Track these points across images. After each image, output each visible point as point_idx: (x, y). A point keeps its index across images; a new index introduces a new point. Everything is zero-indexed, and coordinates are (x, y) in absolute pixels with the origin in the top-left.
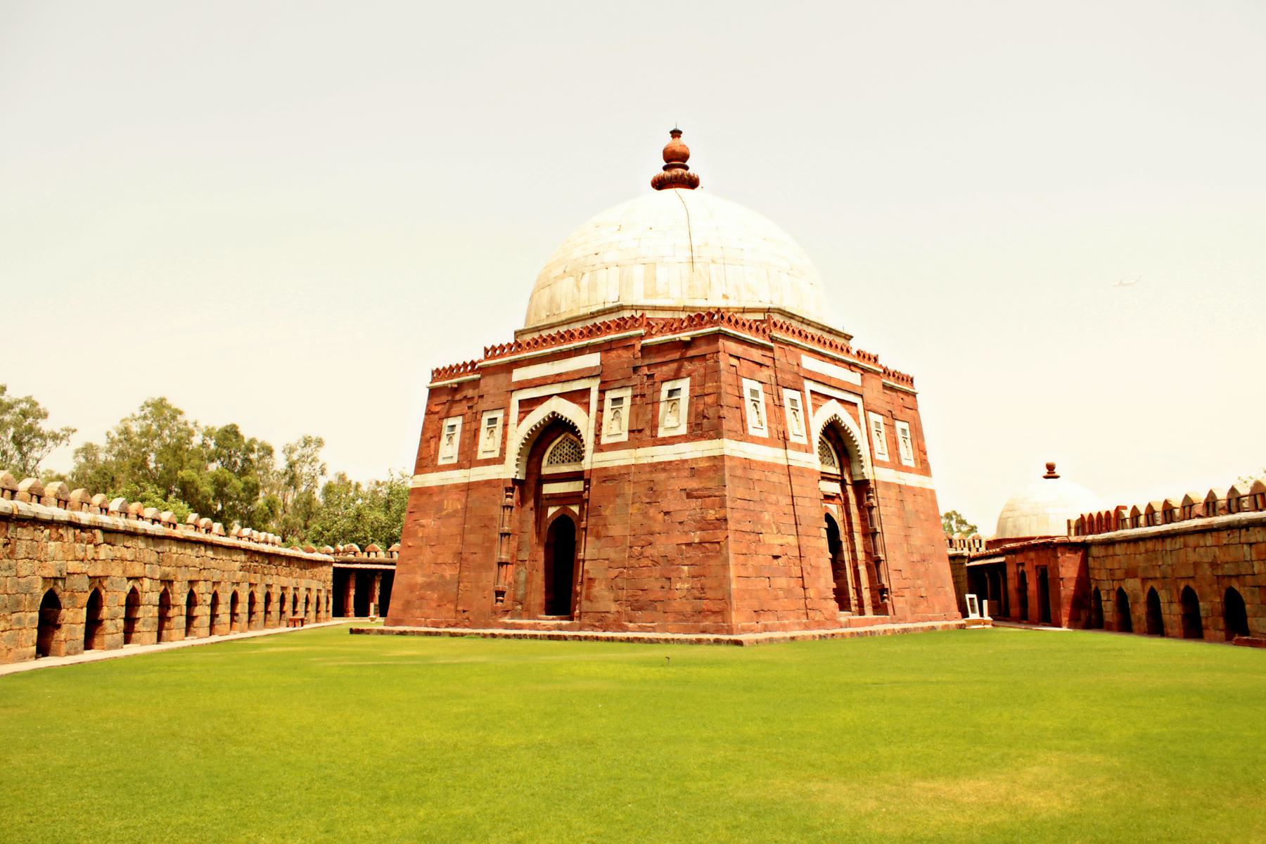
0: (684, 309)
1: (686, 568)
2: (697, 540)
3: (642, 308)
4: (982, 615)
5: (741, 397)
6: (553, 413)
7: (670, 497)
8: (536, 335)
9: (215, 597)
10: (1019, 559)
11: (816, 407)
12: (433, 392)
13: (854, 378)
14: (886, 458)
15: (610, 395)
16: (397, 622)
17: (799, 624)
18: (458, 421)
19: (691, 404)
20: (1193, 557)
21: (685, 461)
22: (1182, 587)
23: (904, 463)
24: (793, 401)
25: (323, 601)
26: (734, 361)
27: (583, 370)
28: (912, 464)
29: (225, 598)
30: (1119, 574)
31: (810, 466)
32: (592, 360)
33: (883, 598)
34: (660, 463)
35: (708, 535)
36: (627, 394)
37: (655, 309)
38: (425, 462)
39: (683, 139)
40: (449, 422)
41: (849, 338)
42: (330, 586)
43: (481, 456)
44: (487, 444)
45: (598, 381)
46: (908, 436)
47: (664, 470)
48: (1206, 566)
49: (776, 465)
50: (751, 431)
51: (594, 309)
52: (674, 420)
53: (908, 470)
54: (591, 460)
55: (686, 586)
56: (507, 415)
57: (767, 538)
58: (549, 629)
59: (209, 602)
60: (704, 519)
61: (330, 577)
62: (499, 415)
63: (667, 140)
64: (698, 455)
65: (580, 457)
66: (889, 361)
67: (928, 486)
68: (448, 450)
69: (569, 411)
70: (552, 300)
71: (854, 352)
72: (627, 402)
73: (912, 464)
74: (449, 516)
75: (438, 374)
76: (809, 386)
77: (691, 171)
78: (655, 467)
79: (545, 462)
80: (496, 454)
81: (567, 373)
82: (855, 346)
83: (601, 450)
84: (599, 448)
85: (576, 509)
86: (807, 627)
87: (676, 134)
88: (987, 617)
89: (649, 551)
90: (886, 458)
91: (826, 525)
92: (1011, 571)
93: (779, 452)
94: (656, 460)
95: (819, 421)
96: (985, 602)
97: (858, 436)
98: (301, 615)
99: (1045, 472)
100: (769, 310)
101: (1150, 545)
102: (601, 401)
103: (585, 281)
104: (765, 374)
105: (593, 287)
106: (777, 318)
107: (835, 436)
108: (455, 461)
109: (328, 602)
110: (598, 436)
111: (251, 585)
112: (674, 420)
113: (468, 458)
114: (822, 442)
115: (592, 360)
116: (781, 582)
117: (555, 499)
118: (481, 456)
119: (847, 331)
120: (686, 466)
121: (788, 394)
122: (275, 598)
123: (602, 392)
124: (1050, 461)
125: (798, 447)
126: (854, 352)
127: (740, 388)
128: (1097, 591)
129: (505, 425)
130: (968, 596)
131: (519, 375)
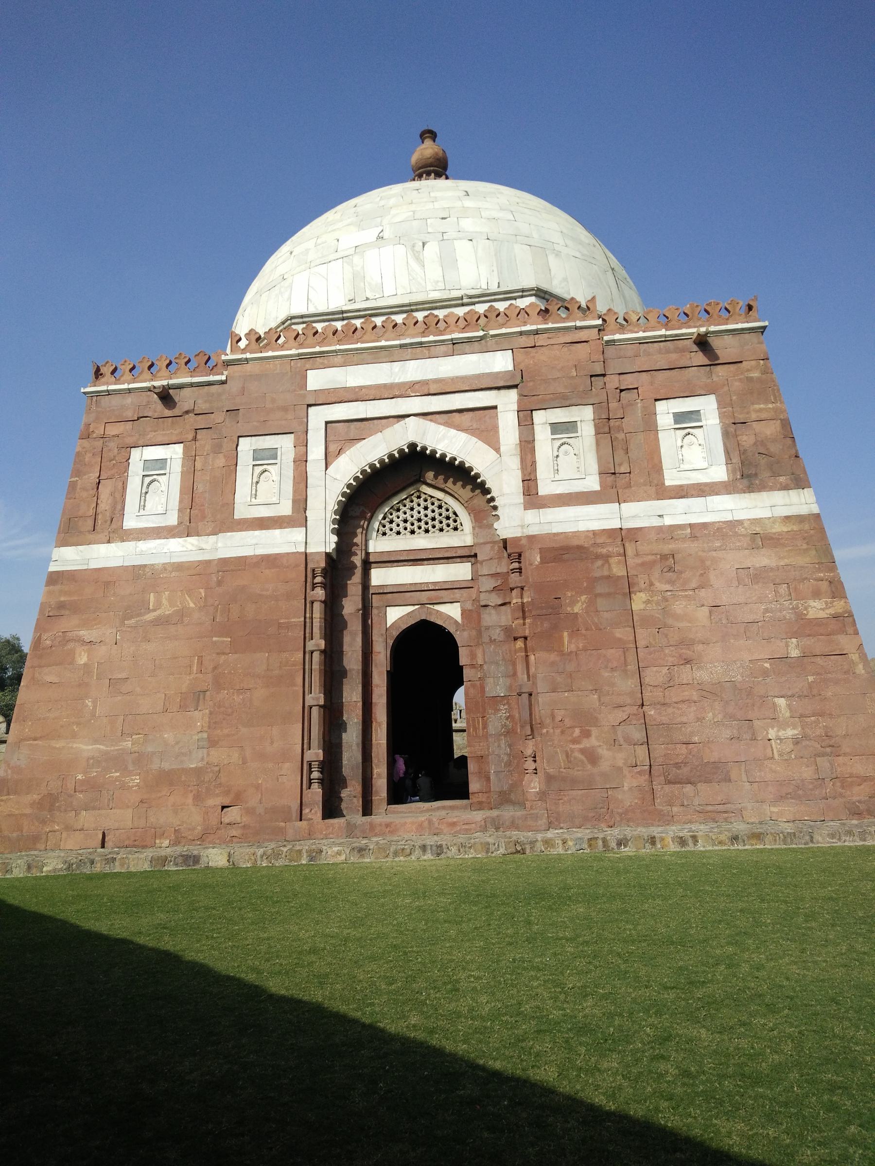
1: (782, 702)
2: (795, 653)
6: (413, 446)
19: (726, 434)
32: (501, 362)
35: (818, 645)
36: (584, 416)
40: (138, 457)
43: (242, 511)
45: (513, 394)
47: (694, 537)
54: (513, 520)
55: (790, 732)
56: (302, 444)
60: (800, 616)
62: (285, 444)
70: (358, 277)
72: (587, 430)
80: (286, 509)
89: (685, 674)
94: (668, 521)
103: (432, 250)
105: (448, 261)
108: (172, 519)
115: (501, 362)
117: (398, 594)
118: (242, 511)
129: (301, 461)
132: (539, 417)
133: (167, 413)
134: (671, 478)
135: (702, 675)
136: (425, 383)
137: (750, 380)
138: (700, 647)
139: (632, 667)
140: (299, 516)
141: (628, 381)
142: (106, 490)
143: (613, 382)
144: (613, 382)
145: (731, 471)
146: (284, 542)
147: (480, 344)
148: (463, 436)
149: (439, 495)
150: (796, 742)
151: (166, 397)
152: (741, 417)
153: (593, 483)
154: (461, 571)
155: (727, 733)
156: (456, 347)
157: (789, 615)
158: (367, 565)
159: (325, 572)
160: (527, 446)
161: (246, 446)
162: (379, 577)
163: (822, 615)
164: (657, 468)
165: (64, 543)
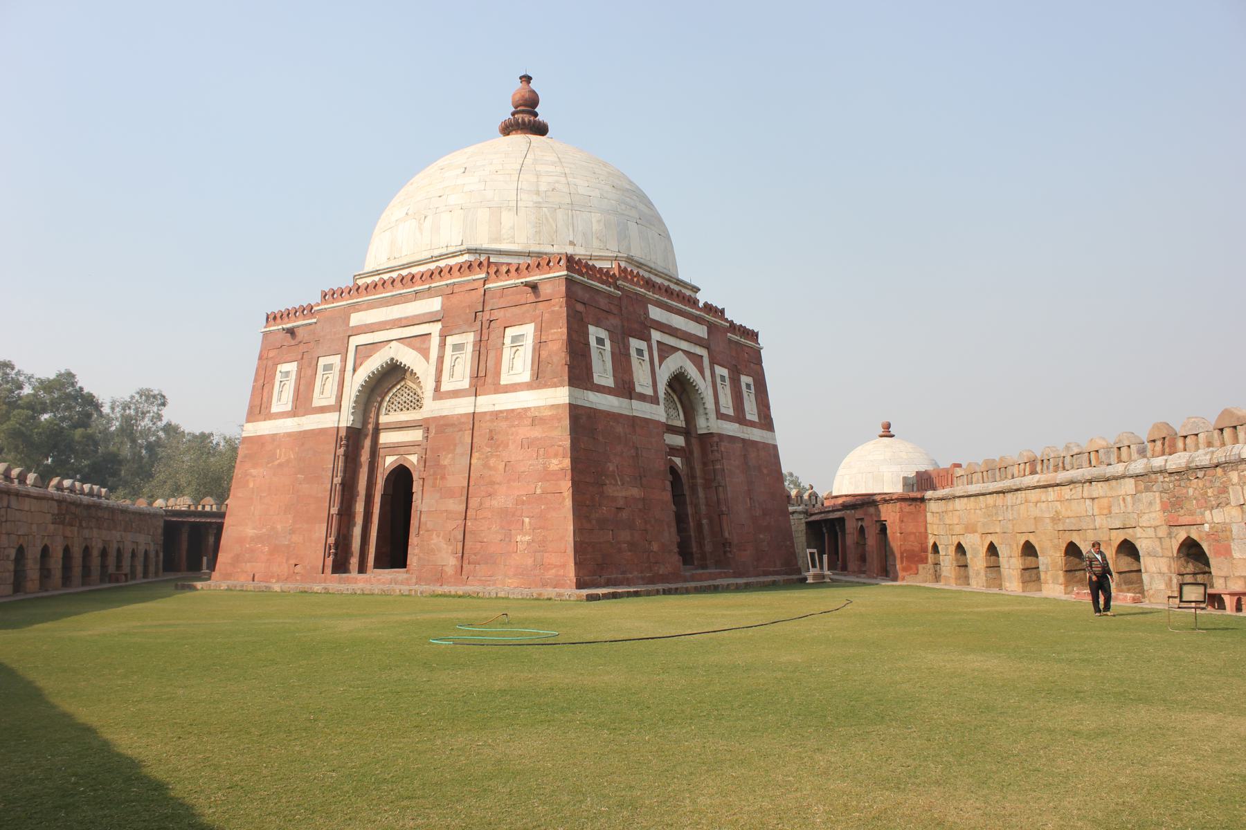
0: (529, 254)
2: (539, 491)
3: (488, 252)
4: (822, 568)
5: (588, 344)
6: (392, 359)
7: (511, 447)
8: (376, 278)
9: (21, 551)
10: (859, 514)
11: (662, 359)
12: (265, 334)
13: (701, 331)
14: (731, 412)
15: (450, 340)
16: (227, 576)
17: (643, 578)
18: (292, 367)
19: (534, 349)
20: (1035, 512)
21: (526, 410)
22: (1022, 542)
23: (748, 417)
24: (640, 352)
25: (152, 555)
26: (580, 307)
27: (424, 314)
28: (755, 418)
29: (33, 553)
30: (958, 529)
31: (656, 418)
33: (725, 552)
34: (501, 412)
36: (469, 339)
37: (500, 253)
38: (259, 409)
39: (533, 85)
41: (697, 290)
42: (160, 539)
43: (318, 401)
44: (323, 394)
45: (439, 326)
46: (753, 390)
47: (507, 419)
48: (1048, 521)
49: (621, 415)
50: (597, 380)
51: (436, 253)
52: (517, 363)
53: (752, 424)
54: (431, 408)
55: (527, 538)
56: (344, 360)
57: (610, 490)
58: (384, 583)
59: (13, 556)
60: (545, 469)
61: (160, 531)
62: (336, 360)
63: (518, 85)
64: (541, 403)
65: (417, 403)
66: (735, 315)
67: (770, 442)
68: (282, 399)
69: (407, 357)
71: (701, 305)
72: (469, 348)
73: (755, 418)
74: (280, 465)
75: (272, 318)
76: (656, 335)
77: (540, 118)
78: (496, 415)
79: (383, 411)
81: (406, 318)
82: (702, 298)
83: (441, 399)
84: (438, 393)
85: (414, 459)
86: (651, 581)
87: (527, 79)
88: (827, 572)
89: (487, 503)
90: (731, 412)
91: (670, 477)
92: (851, 526)
93: (625, 402)
94: (497, 408)
95: (665, 373)
96: (825, 557)
97: (703, 386)
98: (126, 569)
99: (881, 431)
100: (616, 258)
101: (990, 500)
102: (443, 345)
104: (614, 321)
106: (623, 264)
107: (679, 384)
108: (289, 408)
109: (157, 555)
110: (438, 381)
111: (65, 537)
112: (517, 363)
113: (302, 404)
114: (667, 393)
116: (625, 535)
118: (318, 401)
119: (693, 283)
120: (529, 414)
121: (635, 343)
122: (95, 553)
123: (443, 337)
124: (886, 420)
125: (642, 397)
126: (701, 305)
127: (586, 334)
128: (935, 546)
129: (343, 370)
130: (808, 551)
131: (356, 319)
132: (449, 340)
133: (293, 342)
134: (505, 380)
135: (495, 503)
136: (400, 319)
137: (553, 312)
138: (496, 487)
139: (464, 498)
140: (338, 407)
141: (497, 314)
142: (266, 390)
143: (487, 316)
144: (487, 316)
145: (532, 375)
146: (328, 421)
147: (430, 293)
148: (415, 352)
149: (414, 386)
150: (529, 543)
151: (291, 332)
152: (544, 339)
153: (465, 384)
154: (416, 435)
155: (500, 537)
156: (417, 295)
157: (540, 467)
158: (377, 430)
159: (348, 437)
160: (441, 359)
161: (323, 361)
162: (385, 438)
163: (556, 468)
164: (498, 374)
165: (248, 421)
